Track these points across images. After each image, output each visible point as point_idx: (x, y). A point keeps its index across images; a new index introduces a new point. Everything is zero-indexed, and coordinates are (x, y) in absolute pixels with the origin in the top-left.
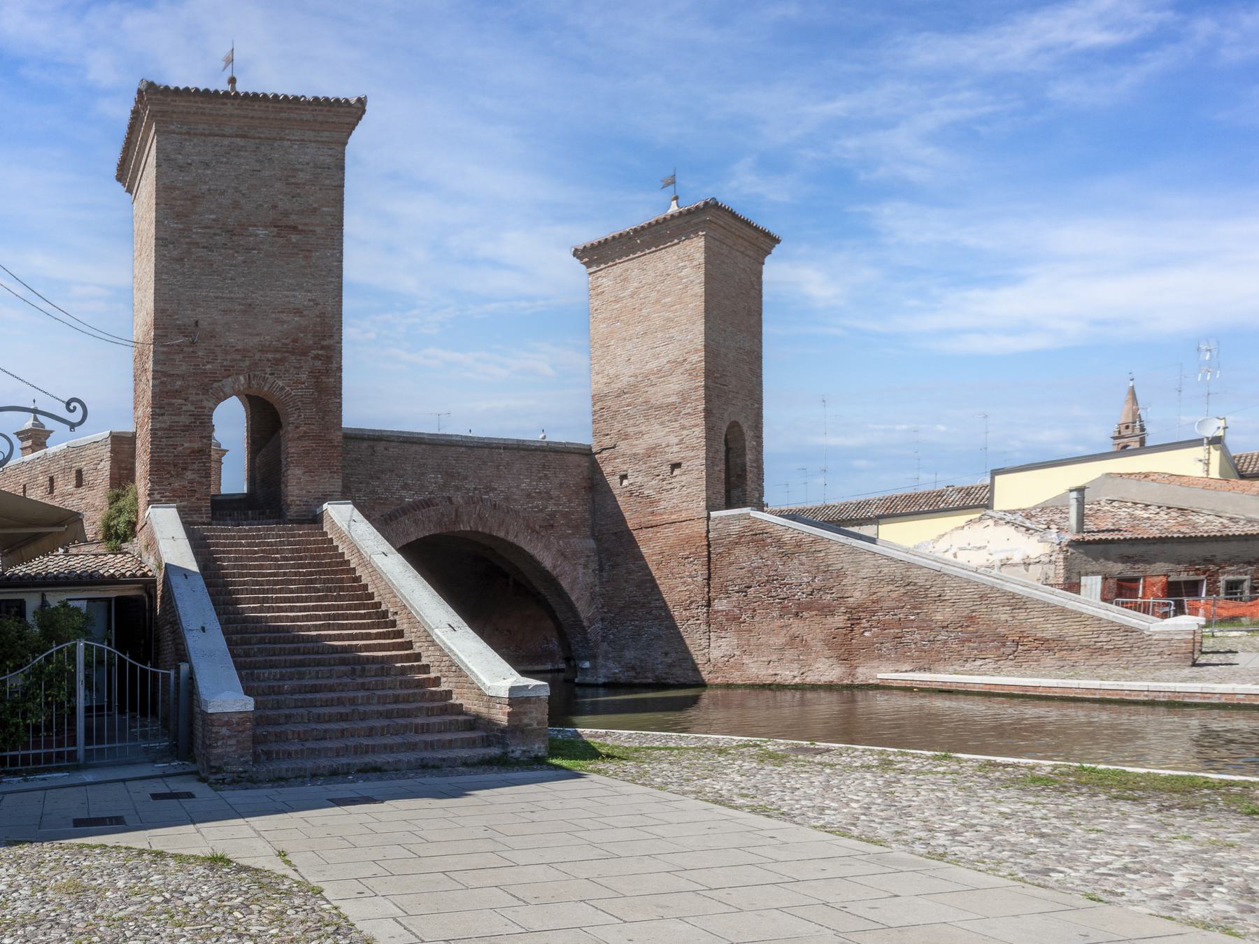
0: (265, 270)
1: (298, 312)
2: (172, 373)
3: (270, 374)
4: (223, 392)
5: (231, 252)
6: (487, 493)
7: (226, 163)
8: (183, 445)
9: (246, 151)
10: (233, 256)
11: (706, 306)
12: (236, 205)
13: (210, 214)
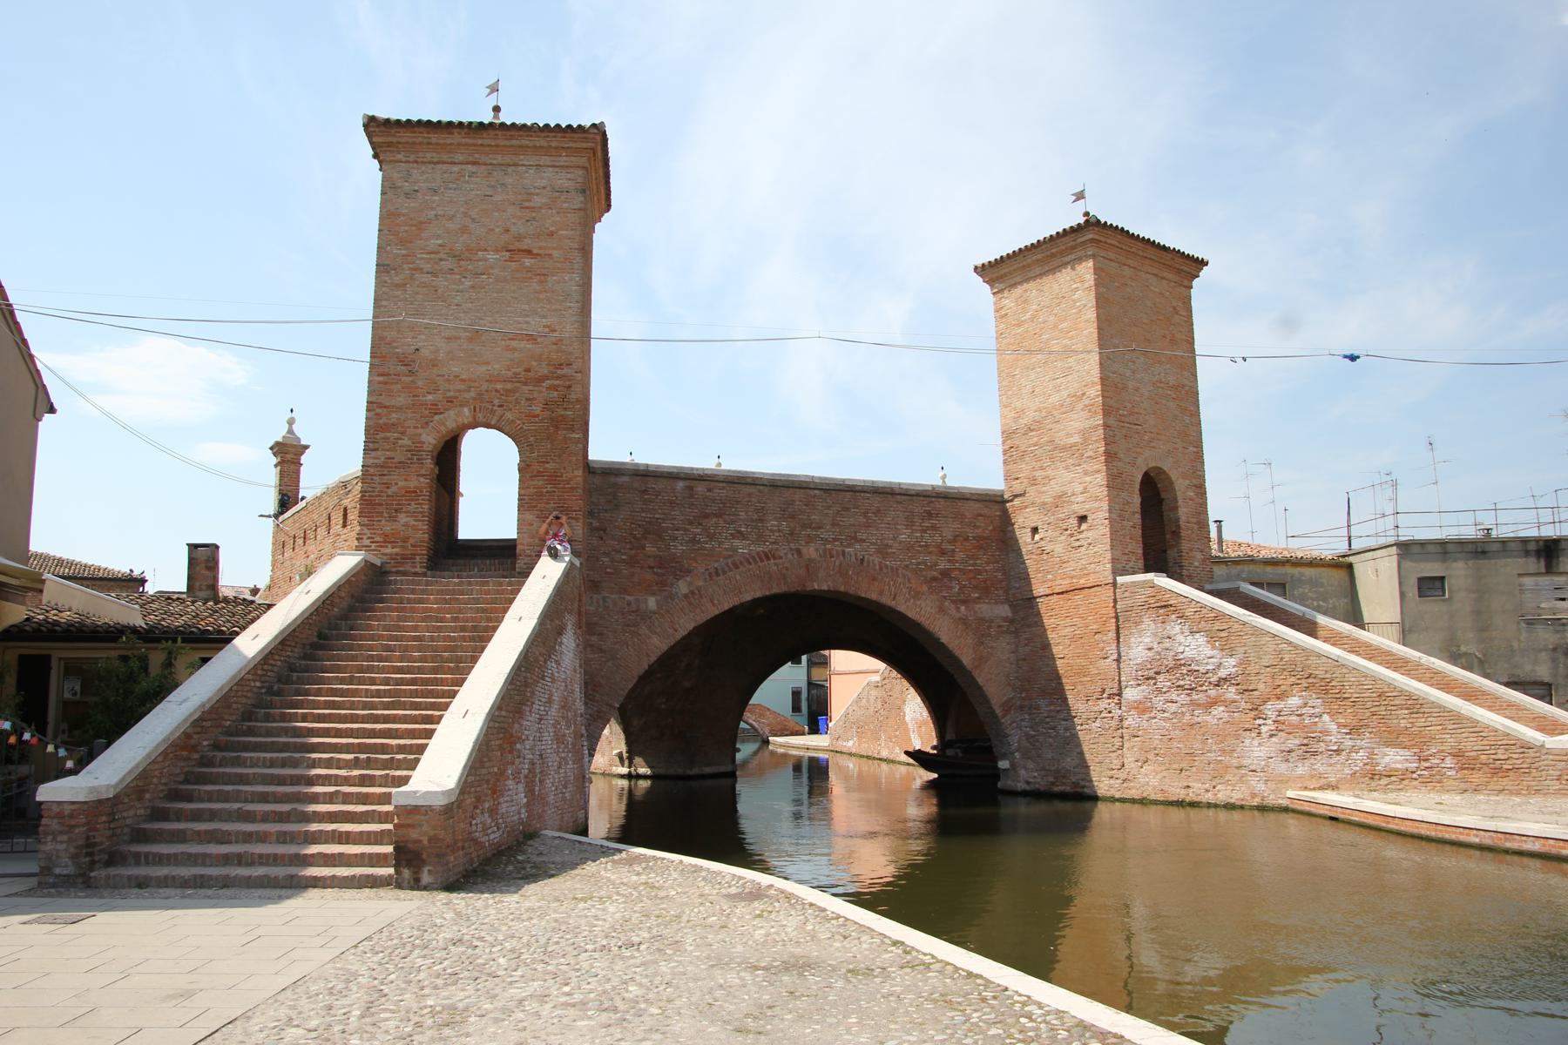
0: (495, 295)
1: (531, 338)
2: (388, 404)
3: (499, 406)
4: (445, 425)
5: (458, 277)
6: (849, 545)
7: (455, 189)
8: (396, 484)
9: (477, 177)
10: (460, 281)
11: (1099, 333)
12: (464, 230)
13: (437, 239)
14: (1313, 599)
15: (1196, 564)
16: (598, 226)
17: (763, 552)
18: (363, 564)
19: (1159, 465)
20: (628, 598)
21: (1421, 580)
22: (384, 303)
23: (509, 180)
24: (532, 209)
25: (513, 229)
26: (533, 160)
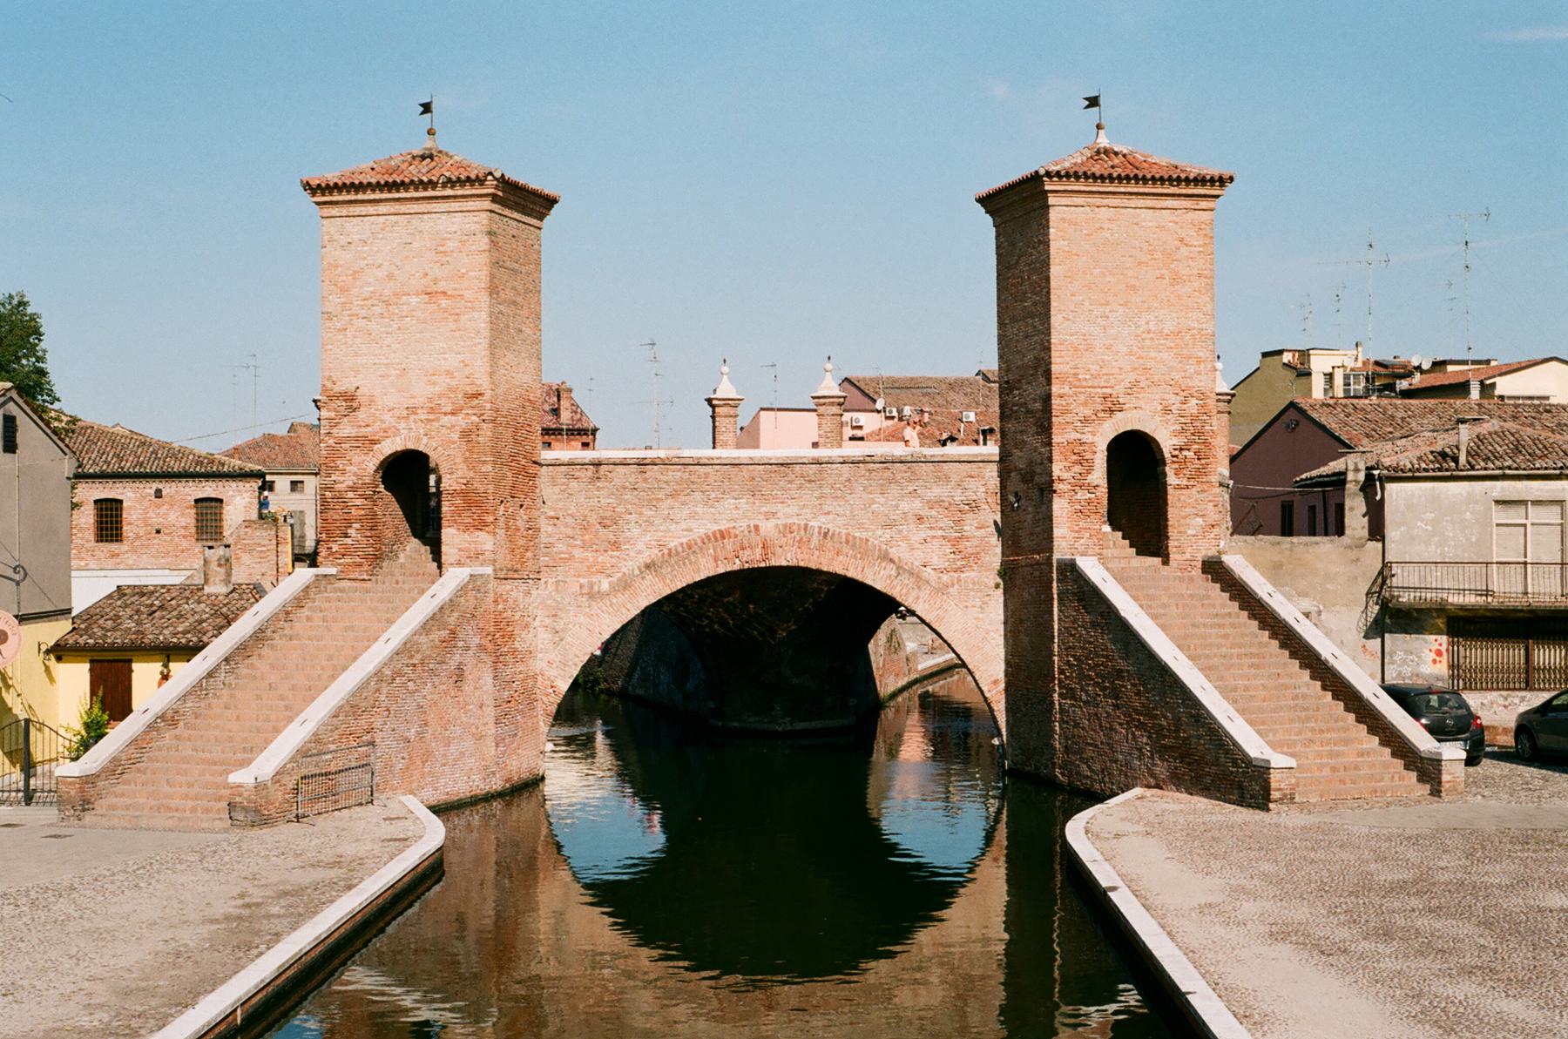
1: (448, 373)
3: (426, 435)
12: (390, 277)
15: (1190, 532)
17: (721, 532)
18: (314, 578)
20: (582, 581)
22: (330, 347)
25: (431, 273)
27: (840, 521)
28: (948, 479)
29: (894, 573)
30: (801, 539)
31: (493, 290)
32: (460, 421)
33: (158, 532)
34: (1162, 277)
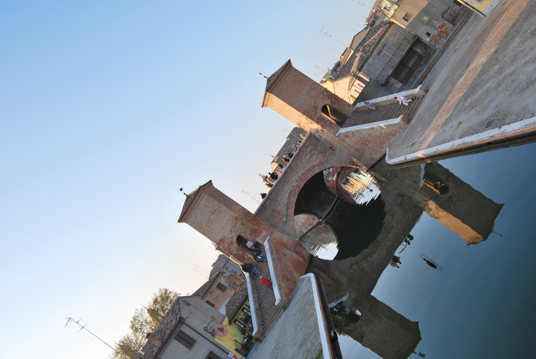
1: (229, 220)
12: (205, 218)
14: (394, 39)
15: (347, 109)
16: (214, 185)
17: (289, 193)
19: (322, 106)
20: (281, 223)
21: (404, 18)
23: (200, 206)
24: (207, 206)
25: (209, 211)
26: (199, 200)
27: (302, 170)
28: (308, 146)
29: (318, 167)
30: (301, 179)
31: (220, 202)
32: (239, 224)
33: (217, 298)
34: (299, 84)
